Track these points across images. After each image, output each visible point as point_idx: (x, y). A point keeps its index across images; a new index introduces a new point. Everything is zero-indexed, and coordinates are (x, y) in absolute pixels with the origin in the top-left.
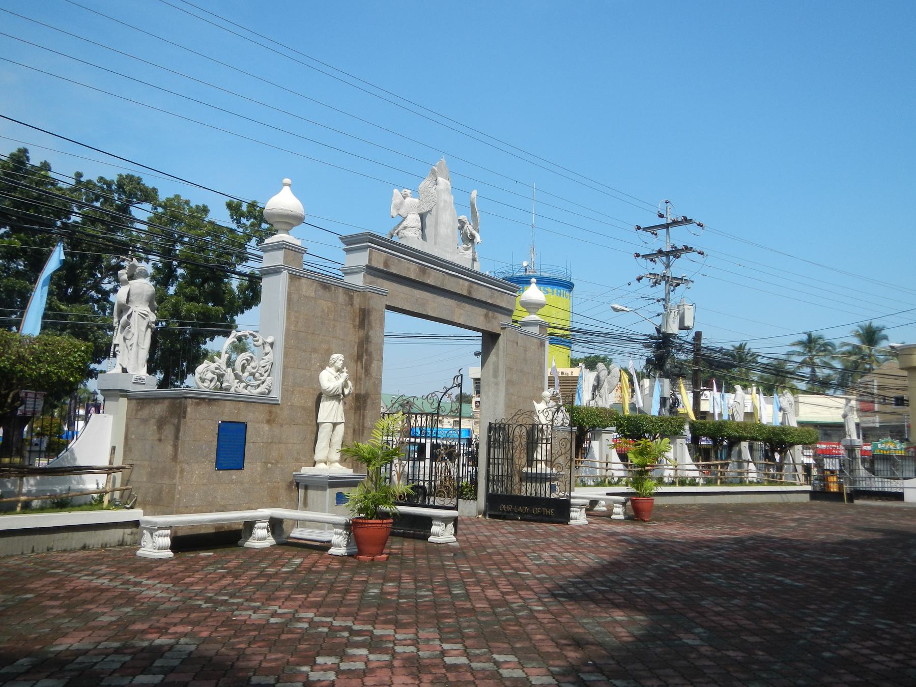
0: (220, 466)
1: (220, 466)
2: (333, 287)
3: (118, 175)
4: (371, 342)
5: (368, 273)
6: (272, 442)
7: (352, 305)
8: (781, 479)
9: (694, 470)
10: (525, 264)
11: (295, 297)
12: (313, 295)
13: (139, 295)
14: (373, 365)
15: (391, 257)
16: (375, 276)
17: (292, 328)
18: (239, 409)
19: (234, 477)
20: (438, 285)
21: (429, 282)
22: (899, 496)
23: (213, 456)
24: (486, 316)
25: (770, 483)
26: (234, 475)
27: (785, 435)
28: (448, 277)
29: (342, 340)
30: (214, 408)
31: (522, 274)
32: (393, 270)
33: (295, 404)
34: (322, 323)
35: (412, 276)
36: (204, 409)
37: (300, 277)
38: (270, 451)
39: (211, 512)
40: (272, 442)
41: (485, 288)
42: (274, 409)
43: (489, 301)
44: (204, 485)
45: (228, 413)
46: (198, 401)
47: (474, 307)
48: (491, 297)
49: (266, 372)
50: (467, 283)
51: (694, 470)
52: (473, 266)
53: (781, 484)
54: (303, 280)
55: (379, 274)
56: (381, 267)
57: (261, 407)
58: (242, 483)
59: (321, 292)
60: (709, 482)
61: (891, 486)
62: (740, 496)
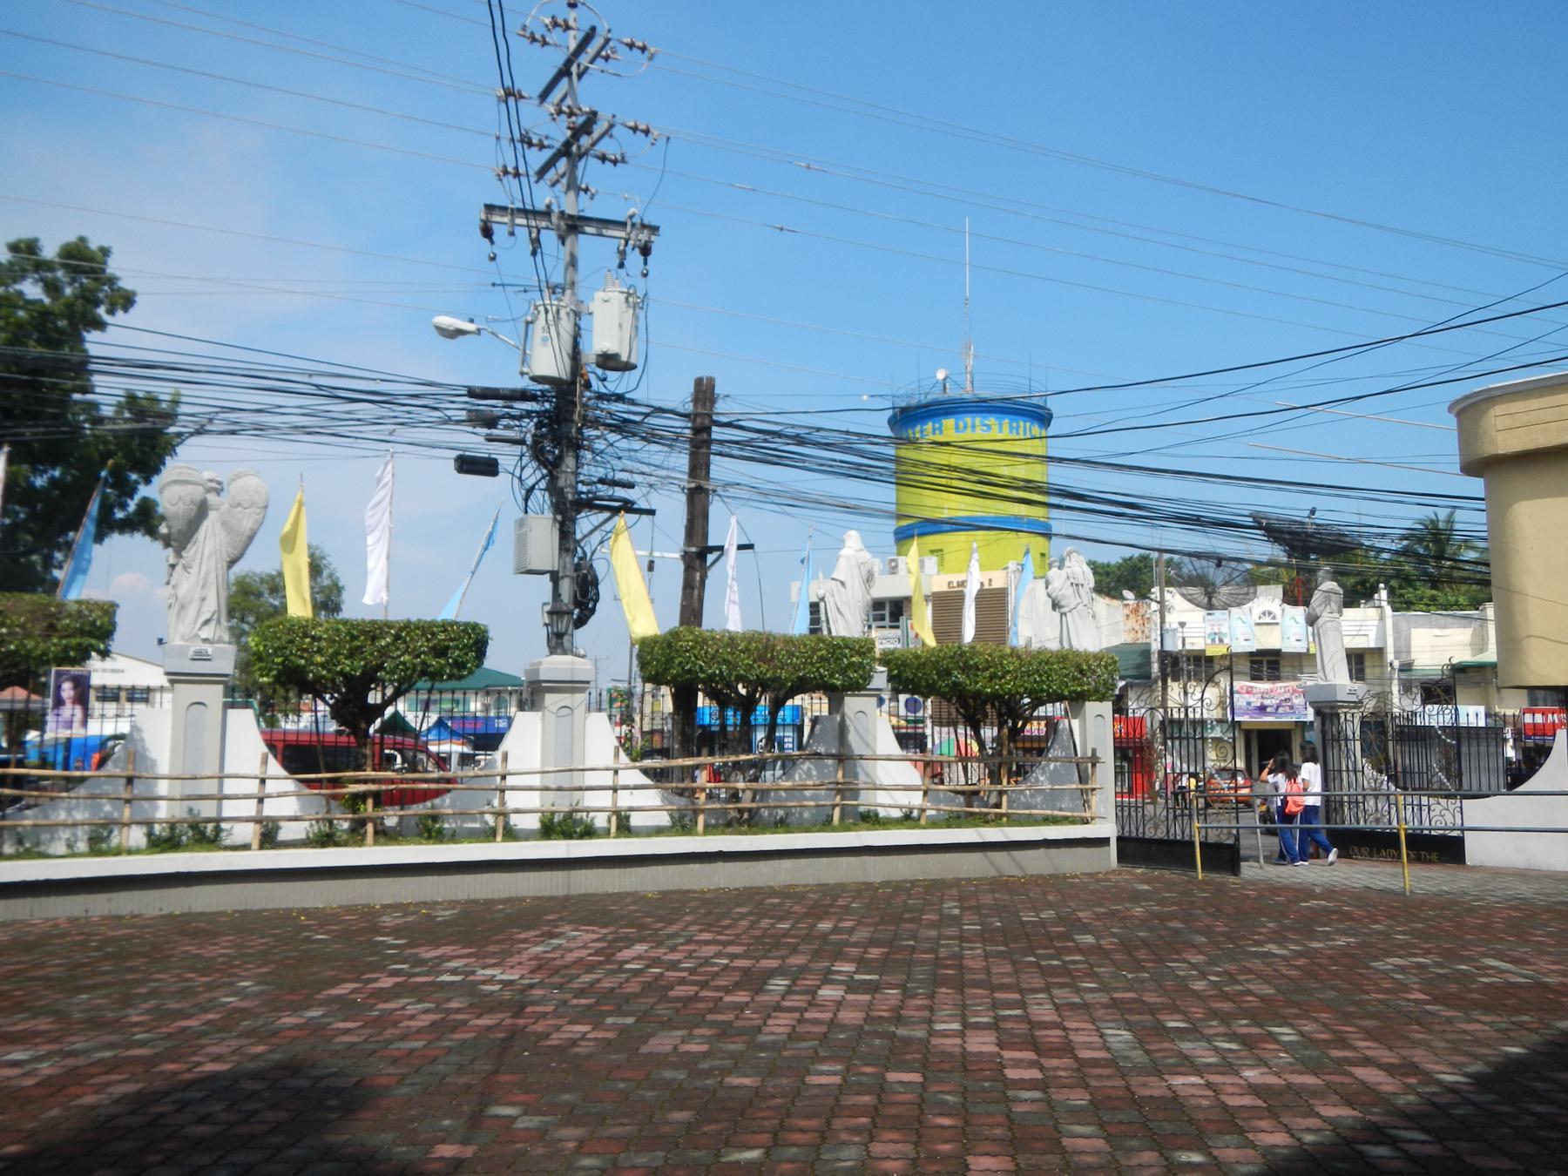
8: (998, 805)
9: (636, 788)
10: (940, 375)
22: (1448, 849)
25: (954, 820)
27: (966, 669)
31: (936, 395)
51: (636, 788)
53: (997, 820)
60: (682, 825)
61: (1439, 816)
62: (787, 864)
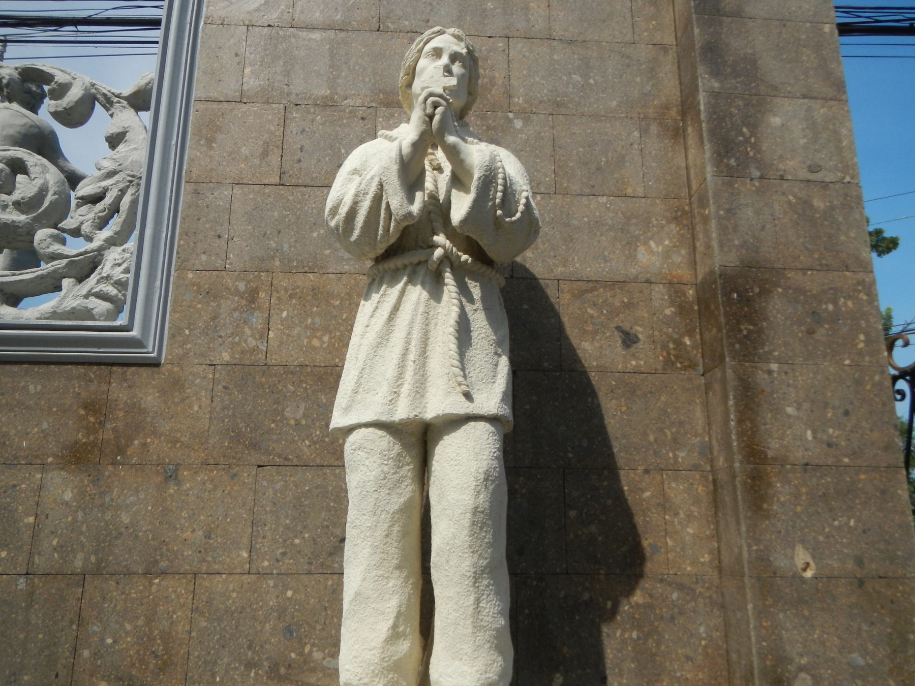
6: (98, 572)
29: (571, 42)
33: (273, 359)
38: (80, 621)
40: (98, 572)
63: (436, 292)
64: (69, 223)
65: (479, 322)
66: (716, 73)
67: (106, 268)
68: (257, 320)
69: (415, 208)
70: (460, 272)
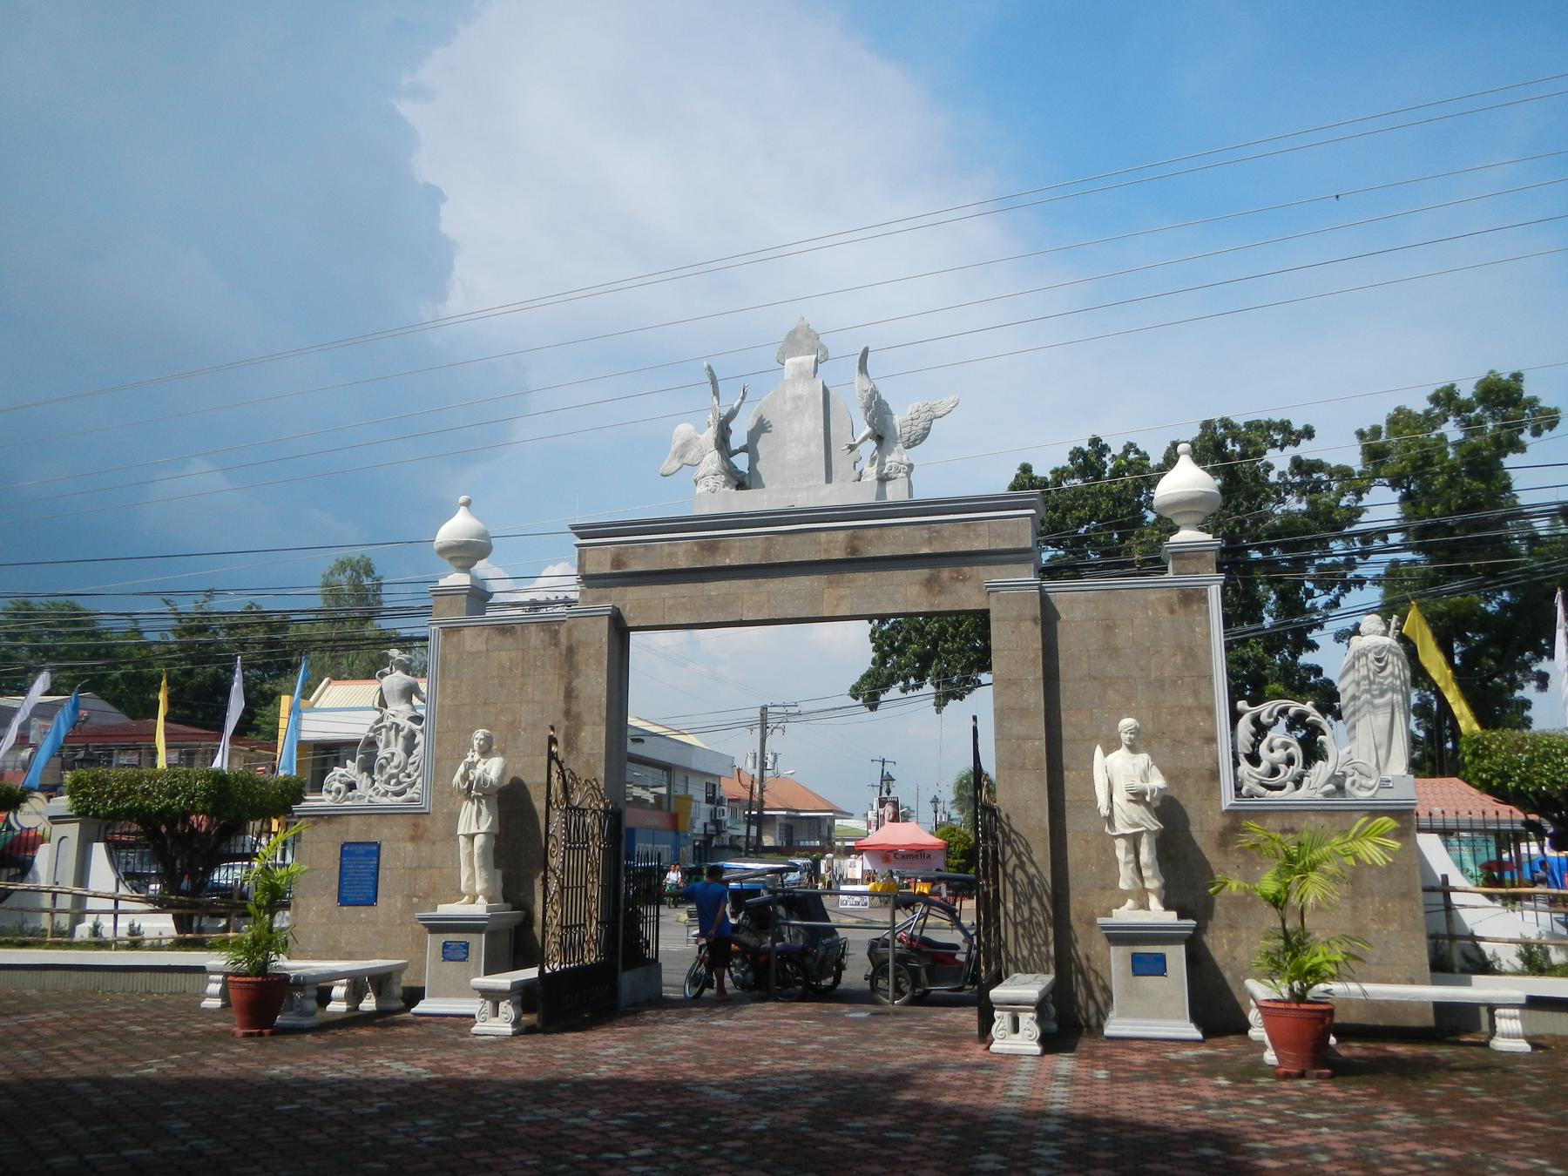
0: (343, 901)
1: (343, 901)
2: (519, 627)
3: (1095, 441)
4: (577, 697)
5: (589, 587)
7: (557, 645)
11: (453, 658)
12: (483, 647)
13: (388, 692)
14: (583, 734)
15: (626, 548)
16: (605, 586)
17: (448, 702)
18: (370, 825)
19: (363, 915)
20: (756, 559)
21: (728, 562)
23: (335, 887)
24: (930, 583)
26: (364, 912)
28: (781, 538)
30: (336, 826)
32: (636, 566)
34: (501, 685)
35: (683, 563)
36: (323, 829)
37: (459, 629)
38: (416, 879)
39: (333, 959)
41: (906, 529)
42: (420, 820)
43: (925, 550)
44: (324, 924)
45: (355, 831)
46: (314, 819)
47: (885, 574)
48: (930, 541)
49: (416, 771)
50: (841, 535)
52: (881, 493)
54: (466, 631)
55: (623, 580)
56: (607, 570)
57: (401, 820)
58: (374, 924)
59: (497, 639)
63: (473, 804)
64: (407, 771)
65: (484, 809)
66: (568, 719)
67: (417, 785)
68: (453, 800)
69: (465, 787)
70: (479, 799)
